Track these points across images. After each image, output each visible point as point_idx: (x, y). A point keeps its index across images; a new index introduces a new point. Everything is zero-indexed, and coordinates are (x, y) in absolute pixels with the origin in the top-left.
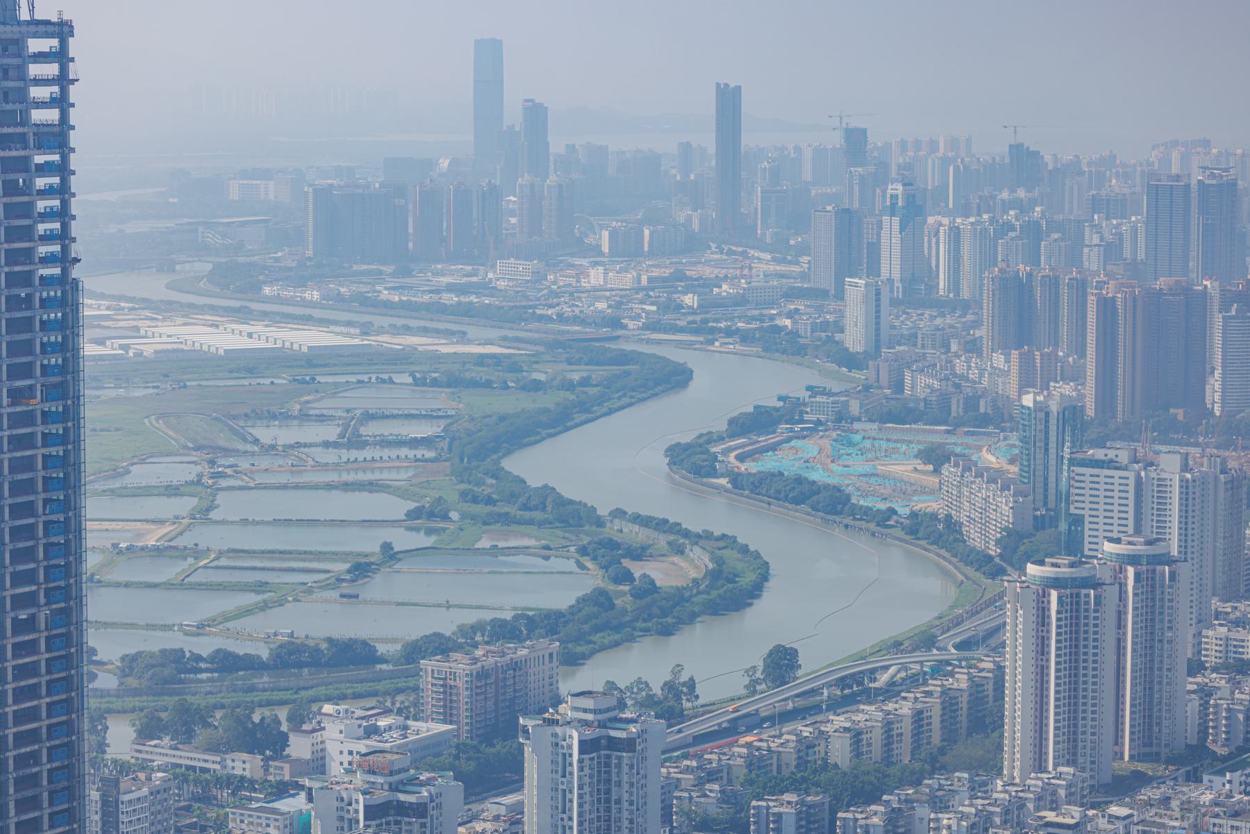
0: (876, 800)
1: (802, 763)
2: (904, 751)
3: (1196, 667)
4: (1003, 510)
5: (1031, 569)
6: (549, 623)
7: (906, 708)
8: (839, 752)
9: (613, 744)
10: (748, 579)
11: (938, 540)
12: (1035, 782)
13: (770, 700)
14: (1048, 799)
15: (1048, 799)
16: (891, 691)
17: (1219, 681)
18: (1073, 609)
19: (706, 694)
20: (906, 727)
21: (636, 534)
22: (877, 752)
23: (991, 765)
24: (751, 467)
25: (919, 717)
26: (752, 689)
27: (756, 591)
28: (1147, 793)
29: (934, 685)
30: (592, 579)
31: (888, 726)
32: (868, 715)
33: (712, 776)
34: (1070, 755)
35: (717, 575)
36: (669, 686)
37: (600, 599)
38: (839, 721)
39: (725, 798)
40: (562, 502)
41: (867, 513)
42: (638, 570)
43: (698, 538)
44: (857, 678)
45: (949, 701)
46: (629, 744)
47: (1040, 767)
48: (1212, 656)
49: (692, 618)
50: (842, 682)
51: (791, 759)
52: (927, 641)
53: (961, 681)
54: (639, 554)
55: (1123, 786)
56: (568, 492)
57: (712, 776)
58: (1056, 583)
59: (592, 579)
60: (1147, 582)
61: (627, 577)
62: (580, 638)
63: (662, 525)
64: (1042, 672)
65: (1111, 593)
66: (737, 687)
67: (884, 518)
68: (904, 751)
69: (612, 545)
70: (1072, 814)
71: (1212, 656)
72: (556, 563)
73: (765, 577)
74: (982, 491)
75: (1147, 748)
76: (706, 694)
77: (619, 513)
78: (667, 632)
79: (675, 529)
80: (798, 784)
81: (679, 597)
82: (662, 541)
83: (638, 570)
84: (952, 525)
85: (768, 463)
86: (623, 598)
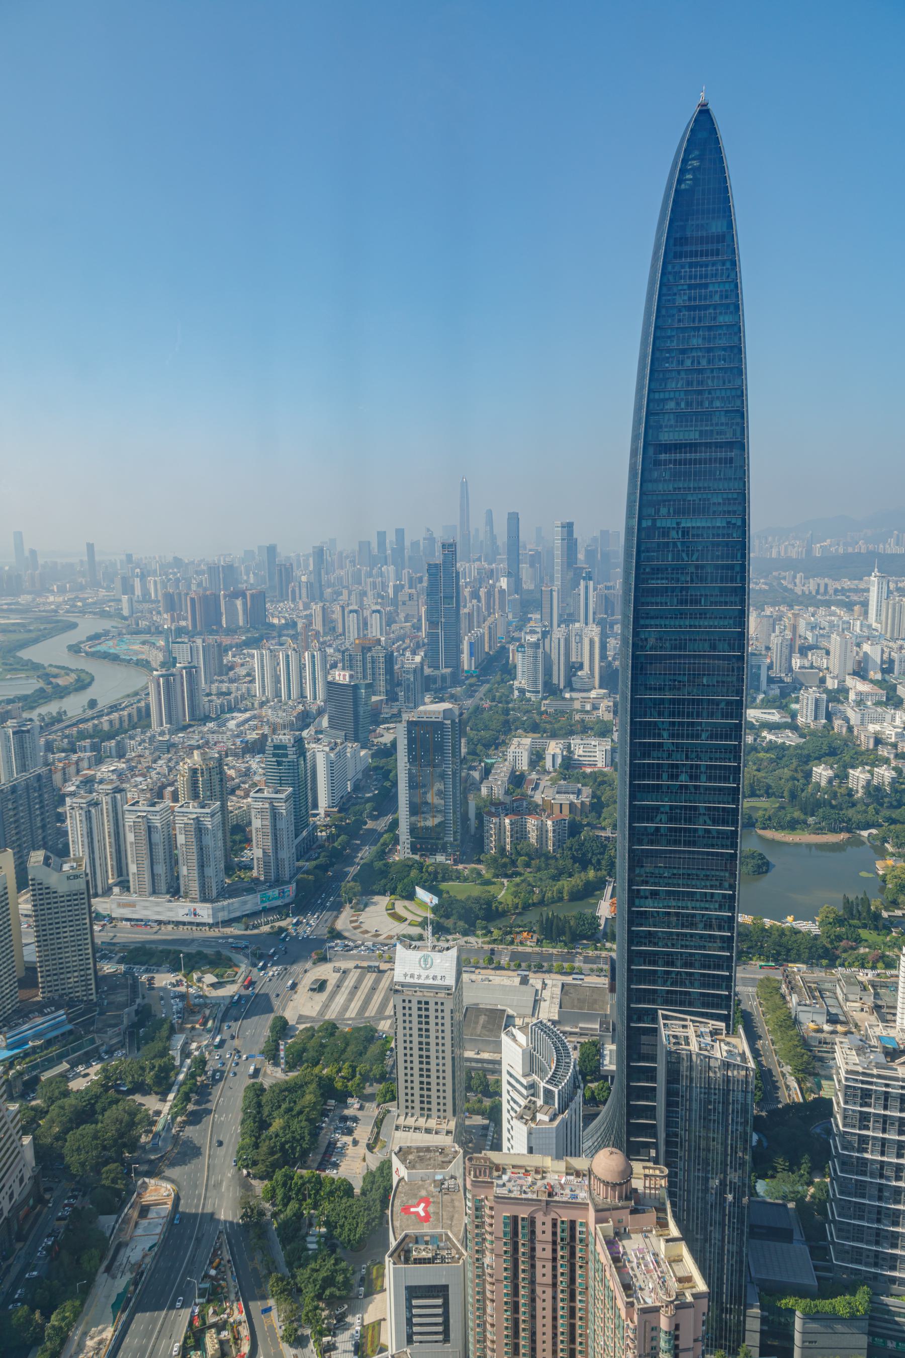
0: (113, 738)
1: (94, 730)
2: (126, 724)
3: (209, 695)
4: (160, 657)
5: (155, 673)
6: (24, 698)
7: (125, 713)
8: (106, 727)
9: (23, 732)
10: (86, 682)
11: (143, 666)
12: (158, 730)
13: (90, 713)
14: (162, 733)
15: (162, 733)
16: (123, 709)
17: (214, 697)
18: (167, 682)
19: (69, 714)
20: (126, 719)
21: (55, 671)
22: (117, 726)
23: (149, 726)
24: (93, 649)
25: (130, 715)
26: (84, 711)
27: (90, 684)
28: (191, 730)
29: (135, 706)
30: (41, 684)
31: (120, 718)
32: (115, 716)
33: (67, 737)
34: (170, 721)
35: (77, 681)
36: (58, 713)
37: (42, 690)
38: (106, 718)
39: (69, 743)
40: (33, 663)
41: (124, 660)
42: (53, 680)
43: (72, 670)
44: (115, 706)
45: (139, 710)
46: (28, 731)
47: (162, 725)
48: (214, 691)
49: (69, 693)
50: (111, 707)
51: (91, 731)
52: (136, 694)
53: (142, 704)
54: (56, 676)
55: (184, 728)
56: (35, 661)
57: (67, 737)
58: (162, 676)
59: (41, 684)
60: (189, 674)
61: (50, 683)
62: (35, 701)
63: (63, 668)
64: (160, 700)
65: (178, 678)
66: (80, 711)
67: (129, 661)
68: (126, 724)
69: (47, 675)
70: (167, 737)
71: (214, 691)
72: (31, 681)
73: (93, 679)
74: (155, 652)
75: (193, 717)
76: (69, 714)
77: (51, 666)
78: (62, 698)
79: (67, 668)
80: (91, 737)
81: (66, 688)
82: (63, 672)
83: (53, 680)
84: (148, 662)
85: (98, 648)
86: (49, 689)
